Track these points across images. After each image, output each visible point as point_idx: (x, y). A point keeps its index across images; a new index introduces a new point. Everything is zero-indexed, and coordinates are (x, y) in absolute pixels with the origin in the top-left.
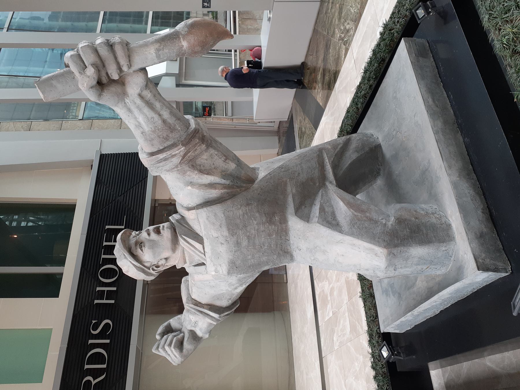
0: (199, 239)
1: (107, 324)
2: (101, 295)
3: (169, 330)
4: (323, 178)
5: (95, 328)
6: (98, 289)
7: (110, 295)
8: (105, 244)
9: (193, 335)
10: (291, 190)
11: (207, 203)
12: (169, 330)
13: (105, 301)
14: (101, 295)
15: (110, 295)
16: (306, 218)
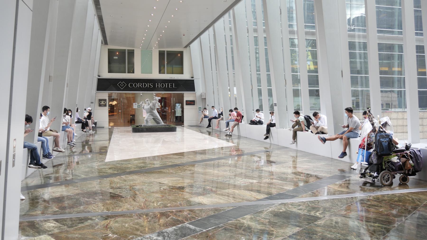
0: (148, 106)
1: (152, 86)
2: (158, 84)
3: (143, 103)
4: (154, 117)
5: (151, 84)
6: (159, 84)
7: (158, 86)
8: (170, 84)
9: (142, 105)
10: (152, 114)
11: (150, 106)
12: (143, 103)
13: (156, 85)
14: (158, 84)
15: (158, 86)
16: (149, 115)
